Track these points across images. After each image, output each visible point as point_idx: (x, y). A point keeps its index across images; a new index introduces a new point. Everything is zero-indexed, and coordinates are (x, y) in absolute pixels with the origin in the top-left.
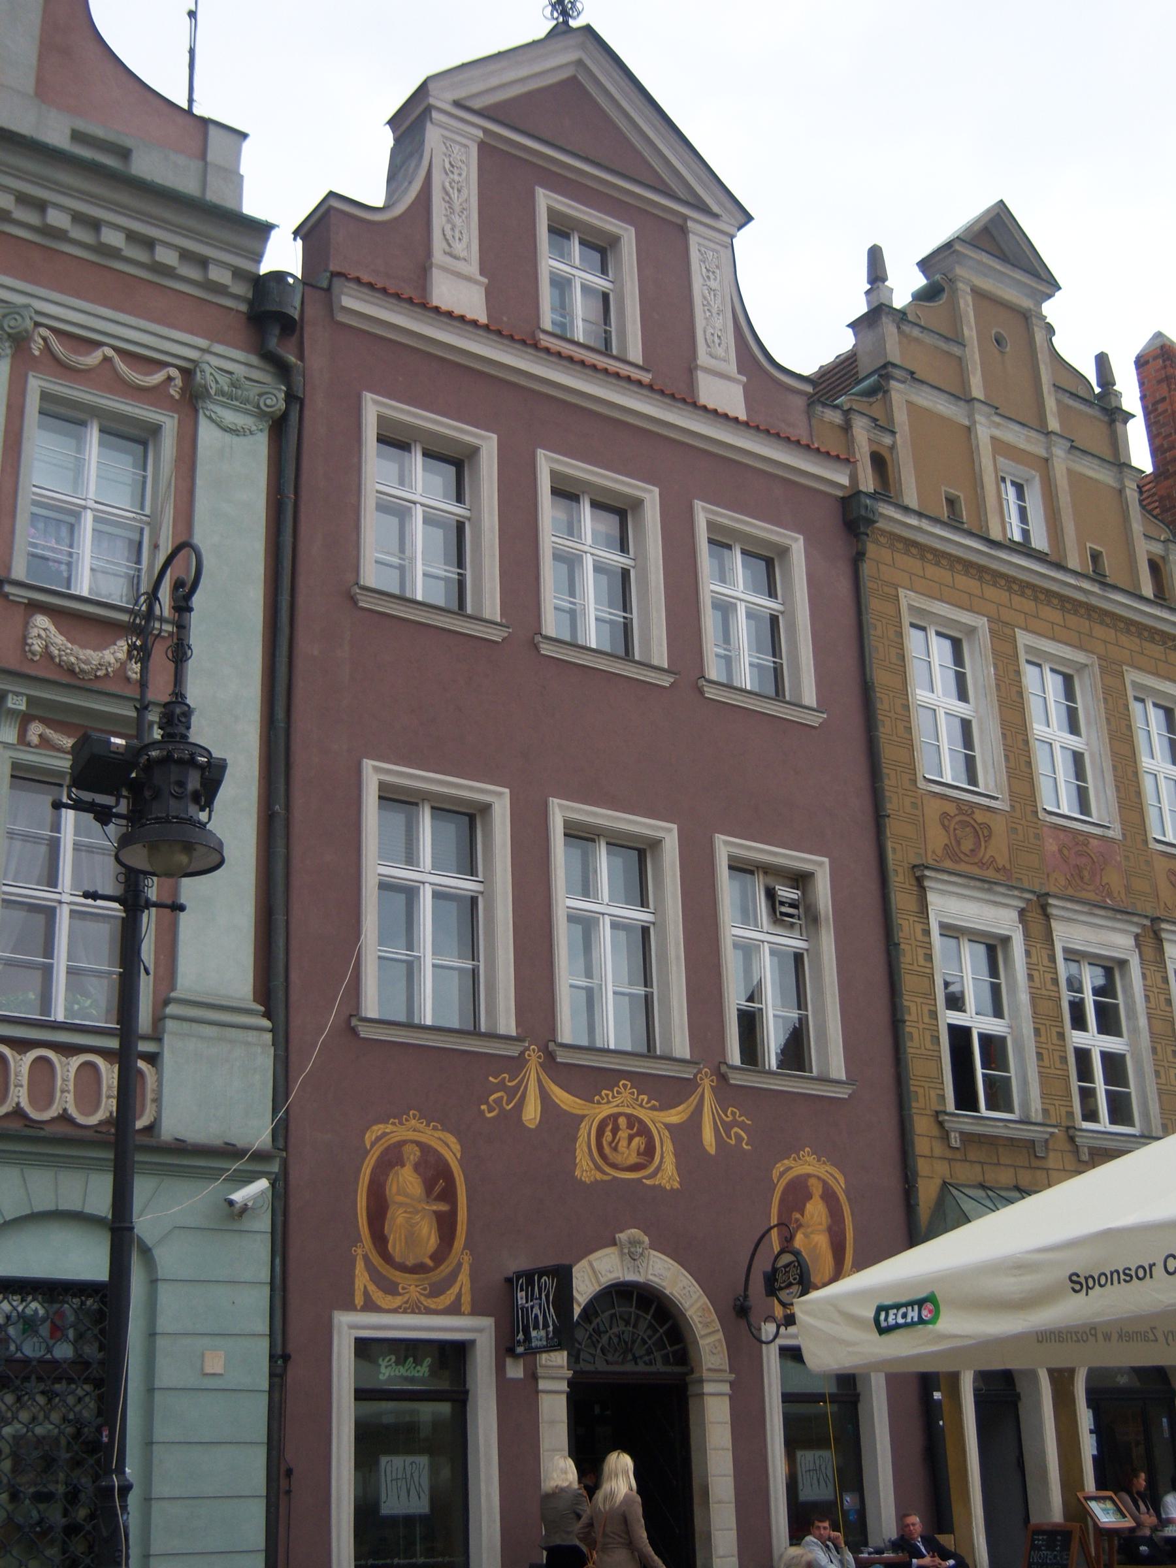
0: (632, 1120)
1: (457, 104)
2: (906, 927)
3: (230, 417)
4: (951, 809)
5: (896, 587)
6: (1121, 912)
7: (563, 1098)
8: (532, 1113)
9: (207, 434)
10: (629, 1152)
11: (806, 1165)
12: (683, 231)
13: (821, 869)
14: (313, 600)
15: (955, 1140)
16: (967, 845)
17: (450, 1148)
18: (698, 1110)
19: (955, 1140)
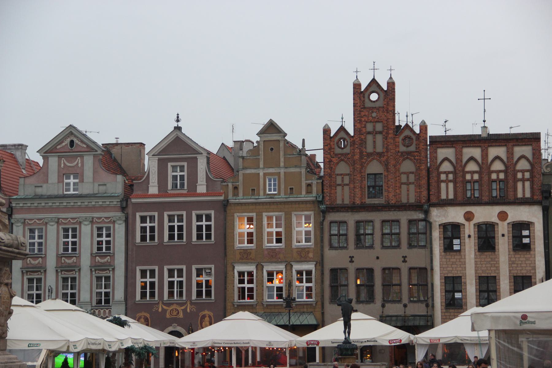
0: (175, 309)
1: (153, 155)
2: (229, 273)
3: (119, 222)
4: (242, 251)
5: (234, 213)
6: (281, 262)
7: (165, 307)
8: (160, 310)
9: (117, 226)
10: (175, 313)
11: (206, 312)
12: (197, 159)
13: (213, 267)
14: (130, 246)
15: (236, 306)
16: (245, 256)
17: (148, 315)
18: (187, 307)
19: (236, 306)
